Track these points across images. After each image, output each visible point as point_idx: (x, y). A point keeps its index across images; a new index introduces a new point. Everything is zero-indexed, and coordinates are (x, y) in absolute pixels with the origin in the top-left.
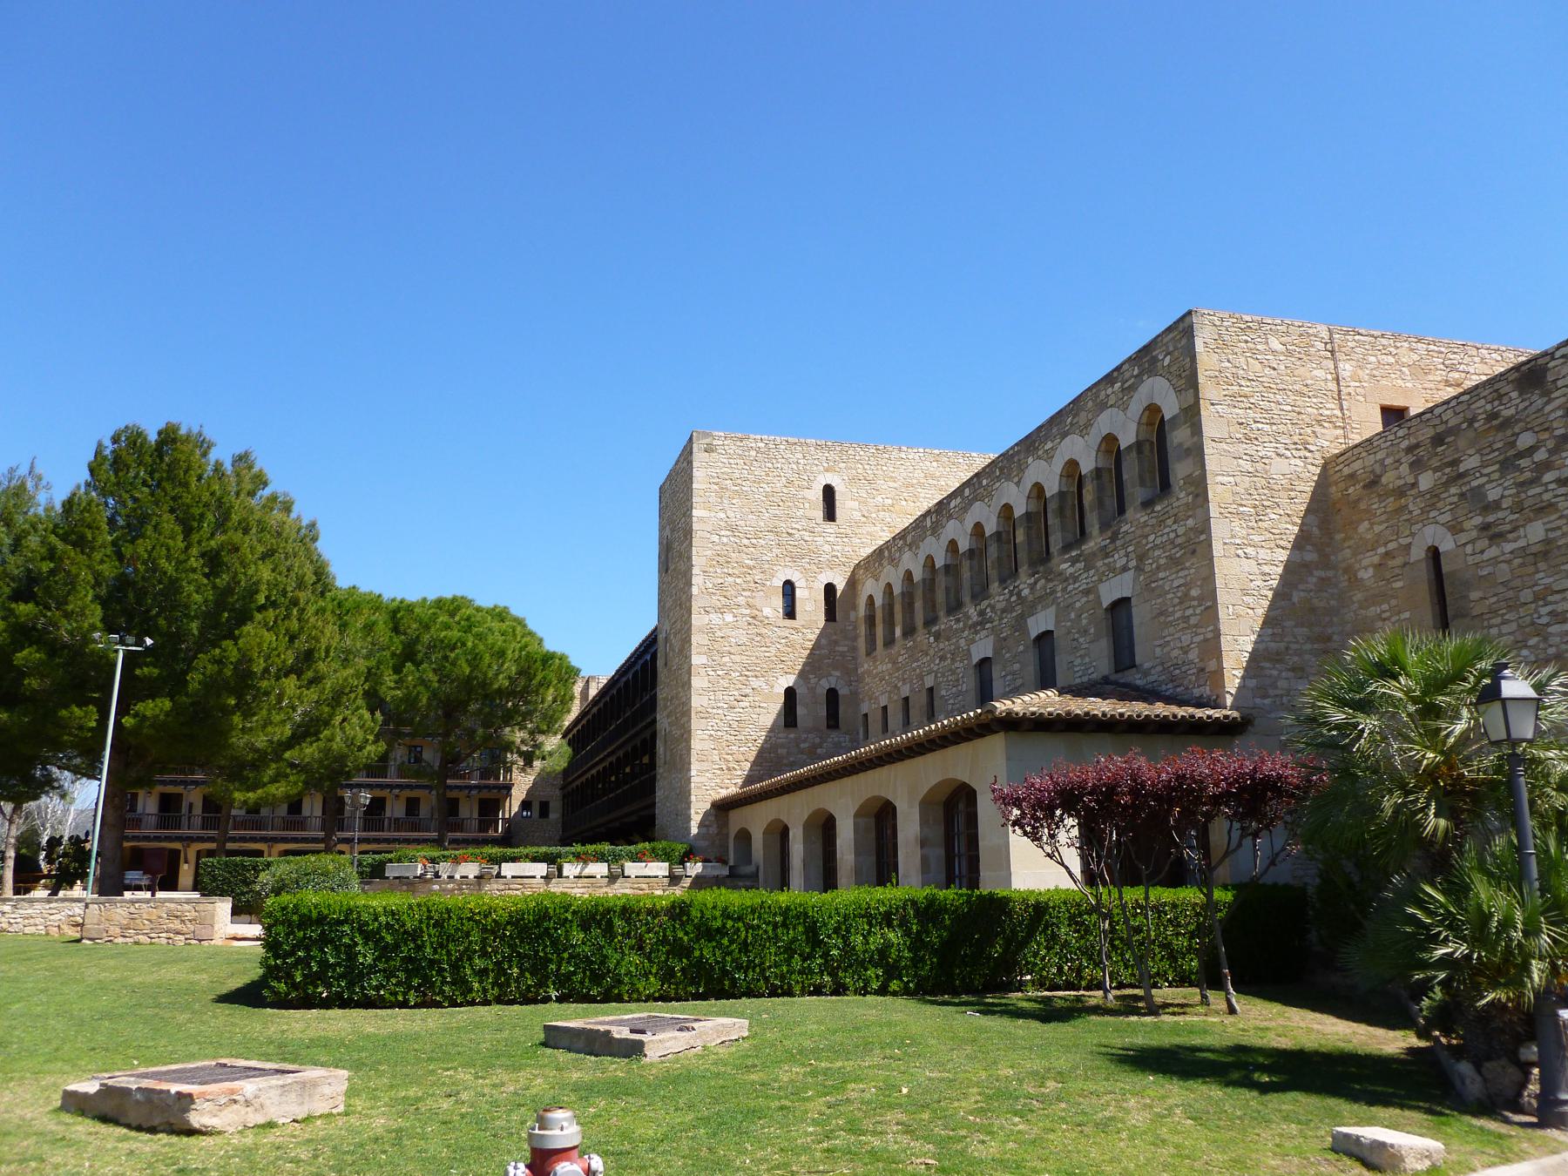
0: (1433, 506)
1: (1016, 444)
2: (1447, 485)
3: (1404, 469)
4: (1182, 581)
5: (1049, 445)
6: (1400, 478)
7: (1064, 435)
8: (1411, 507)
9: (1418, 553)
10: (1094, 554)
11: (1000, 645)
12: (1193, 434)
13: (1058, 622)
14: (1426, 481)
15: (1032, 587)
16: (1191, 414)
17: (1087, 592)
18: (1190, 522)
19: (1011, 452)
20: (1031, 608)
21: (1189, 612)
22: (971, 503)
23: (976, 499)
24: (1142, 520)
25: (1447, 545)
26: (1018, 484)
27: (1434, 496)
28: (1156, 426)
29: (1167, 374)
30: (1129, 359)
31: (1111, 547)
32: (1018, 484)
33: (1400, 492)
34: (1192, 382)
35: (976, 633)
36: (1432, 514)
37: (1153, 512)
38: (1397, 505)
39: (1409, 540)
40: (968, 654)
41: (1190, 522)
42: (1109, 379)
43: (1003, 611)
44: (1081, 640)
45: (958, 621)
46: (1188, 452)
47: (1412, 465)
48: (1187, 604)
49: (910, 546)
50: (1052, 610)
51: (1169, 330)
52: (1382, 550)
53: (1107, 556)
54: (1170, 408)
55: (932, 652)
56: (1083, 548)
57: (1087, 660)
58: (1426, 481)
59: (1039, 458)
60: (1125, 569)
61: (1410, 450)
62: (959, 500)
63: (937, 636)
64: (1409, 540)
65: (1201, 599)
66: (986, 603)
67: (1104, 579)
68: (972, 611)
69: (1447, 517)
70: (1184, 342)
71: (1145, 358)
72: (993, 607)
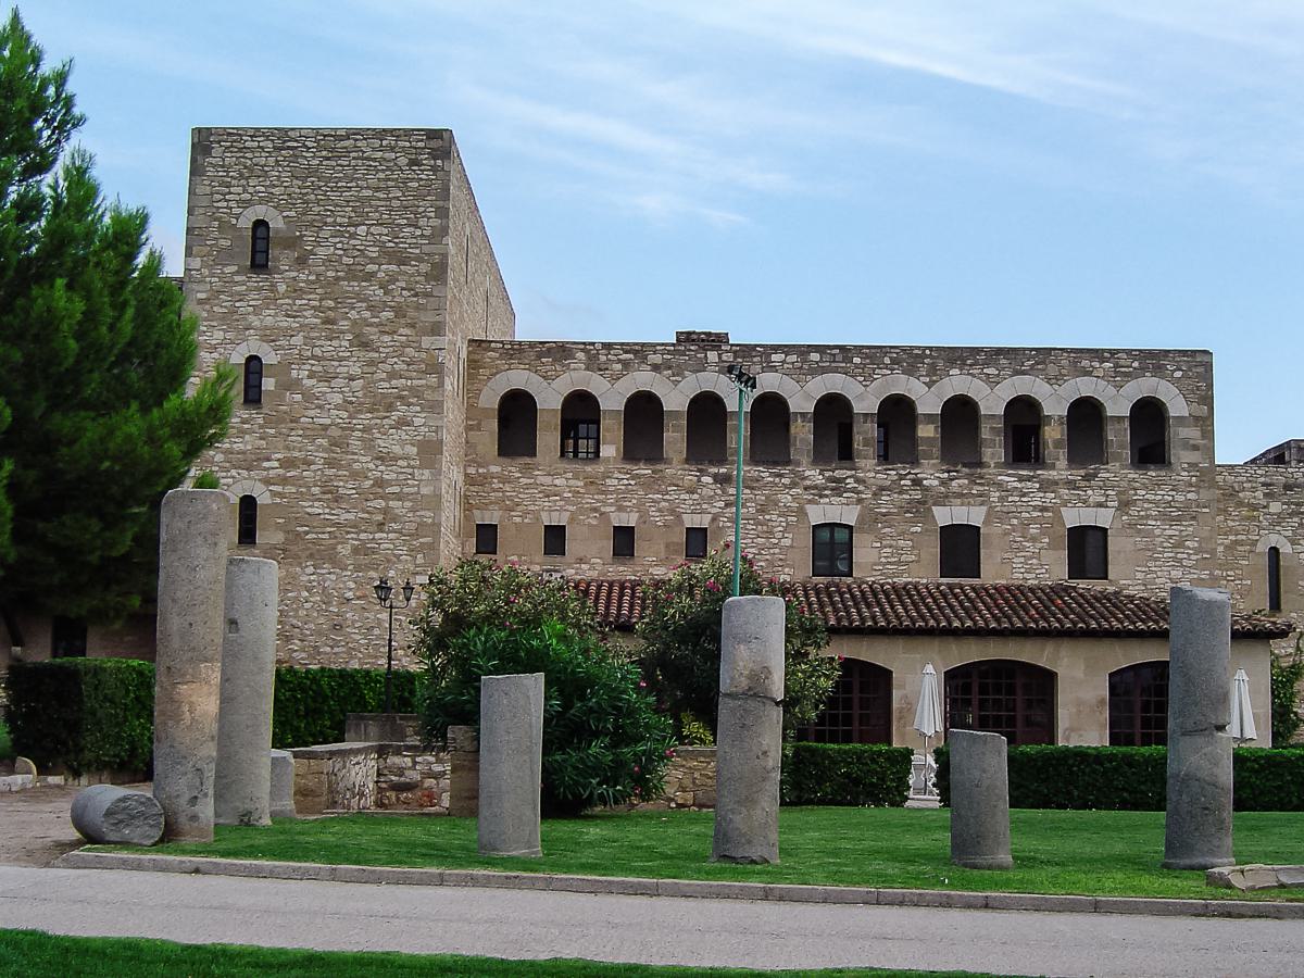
0: (1279, 524)
1: (930, 348)
2: (1291, 515)
3: (1259, 494)
4: (1177, 533)
5: (991, 371)
6: (1255, 498)
7: (1017, 373)
8: (1261, 518)
9: (1263, 548)
10: (1056, 483)
11: (871, 519)
12: (1203, 437)
13: (987, 522)
14: (1275, 507)
15: (943, 483)
16: (1205, 423)
17: (1044, 509)
18: (1189, 496)
19: (916, 351)
20: (943, 500)
21: (1179, 556)
22: (824, 371)
23: (835, 371)
24: (1130, 476)
25: (1286, 549)
26: (929, 385)
27: (1279, 519)
28: (1149, 414)
29: (1174, 381)
30: (1128, 352)
31: (1083, 484)
32: (929, 385)
33: (1254, 508)
34: (1208, 400)
35: (821, 496)
36: (1277, 528)
37: (1146, 474)
38: (1250, 514)
39: (1258, 537)
40: (801, 512)
41: (1189, 496)
42: (1097, 354)
43: (882, 489)
44: (1028, 545)
45: (781, 476)
46: (1196, 448)
47: (1265, 495)
48: (1179, 550)
49: (656, 368)
50: (985, 508)
51: (1184, 353)
52: (1232, 538)
53: (1078, 488)
54: (1177, 406)
55: (706, 492)
56: (1039, 472)
57: (1034, 561)
58: (1275, 507)
59: (973, 375)
60: (1100, 505)
61: (1264, 484)
62: (793, 358)
63: (723, 480)
64: (1258, 537)
65: (1197, 551)
66: (849, 473)
67: (1070, 505)
68: (815, 476)
69: (1290, 533)
70: (1199, 370)
71: (1153, 361)
72: (858, 481)
